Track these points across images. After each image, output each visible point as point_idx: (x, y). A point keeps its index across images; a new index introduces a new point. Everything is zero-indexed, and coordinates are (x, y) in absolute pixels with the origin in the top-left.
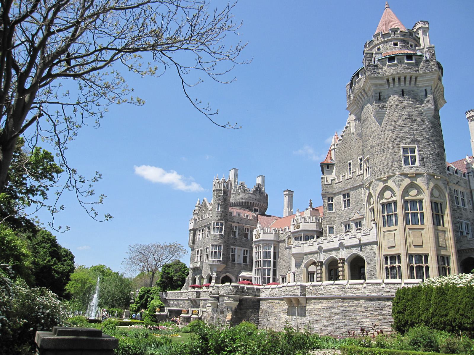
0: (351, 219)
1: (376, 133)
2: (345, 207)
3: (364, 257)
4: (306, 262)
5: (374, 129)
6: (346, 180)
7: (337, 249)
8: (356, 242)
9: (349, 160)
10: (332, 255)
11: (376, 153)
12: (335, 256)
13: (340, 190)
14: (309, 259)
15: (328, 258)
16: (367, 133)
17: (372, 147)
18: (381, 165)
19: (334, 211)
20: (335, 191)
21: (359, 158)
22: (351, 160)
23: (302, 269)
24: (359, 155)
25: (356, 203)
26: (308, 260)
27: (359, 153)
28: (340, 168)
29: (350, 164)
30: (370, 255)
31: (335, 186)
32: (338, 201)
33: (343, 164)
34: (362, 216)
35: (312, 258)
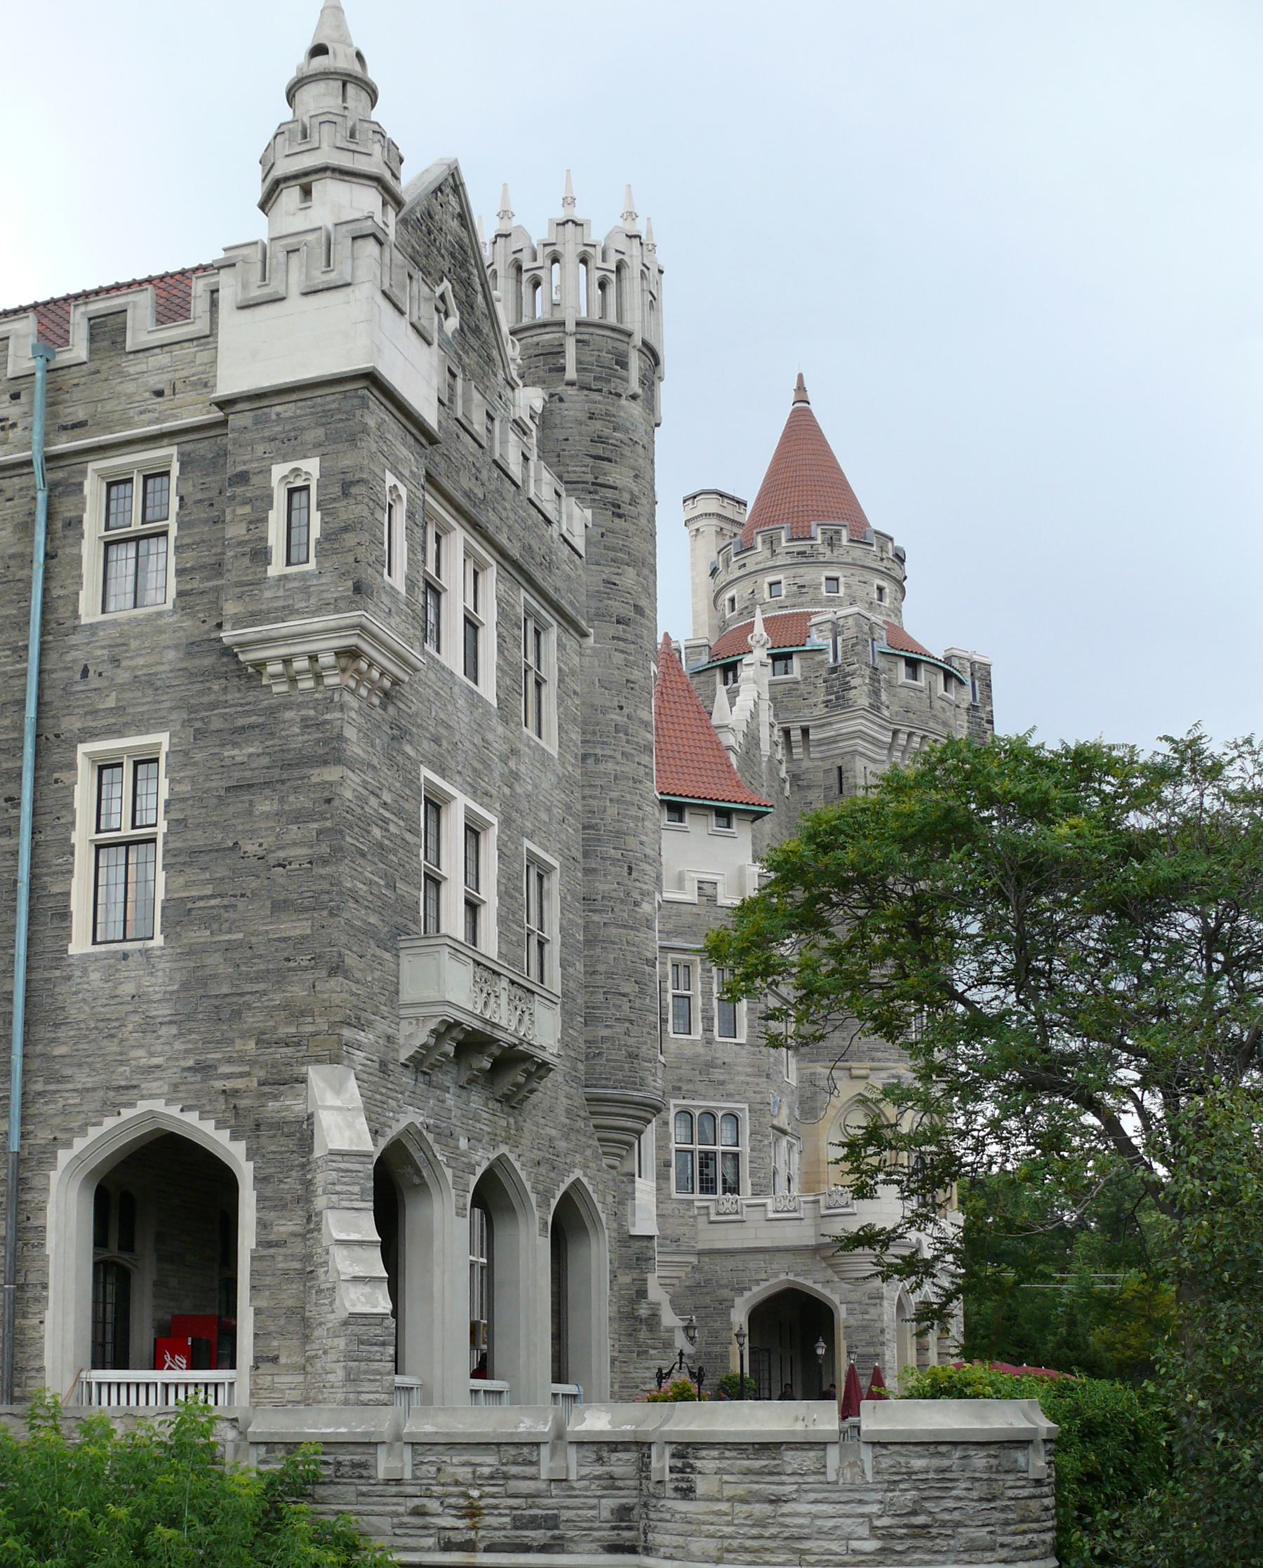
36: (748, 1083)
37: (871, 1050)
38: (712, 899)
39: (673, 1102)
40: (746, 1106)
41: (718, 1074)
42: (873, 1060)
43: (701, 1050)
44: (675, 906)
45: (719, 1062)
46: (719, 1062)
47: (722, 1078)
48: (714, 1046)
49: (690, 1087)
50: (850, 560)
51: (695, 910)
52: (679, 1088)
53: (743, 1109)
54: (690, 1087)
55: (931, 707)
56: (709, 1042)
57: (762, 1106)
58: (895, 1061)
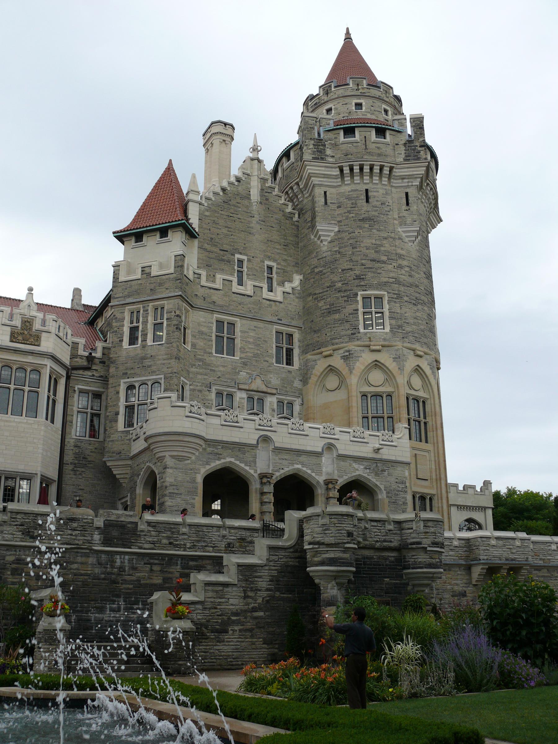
0: (242, 386)
1: (405, 263)
2: (220, 351)
3: (382, 487)
4: (213, 465)
5: (402, 252)
6: (234, 293)
7: (318, 455)
8: (366, 451)
9: (241, 254)
10: (299, 466)
11: (406, 298)
12: (309, 472)
13: (212, 307)
14: (223, 461)
15: (286, 469)
16: (382, 249)
17: (397, 282)
18: (414, 324)
19: (189, 347)
20: (198, 302)
21: (267, 263)
22: (247, 255)
23: (194, 481)
24: (270, 259)
25: (256, 355)
26: (218, 462)
27: (270, 254)
28: (213, 256)
29: (240, 262)
30: (394, 486)
31: (201, 292)
32: (204, 329)
33: (222, 253)
34: (274, 391)
35: (232, 460)
36: (164, 364)
37: (332, 339)
38: (149, 274)
39: (122, 381)
40: (162, 376)
41: (147, 362)
42: (333, 344)
43: (139, 351)
44: (130, 282)
45: (149, 356)
46: (149, 356)
47: (150, 364)
48: (146, 348)
49: (132, 371)
50: (337, 96)
51: (139, 282)
52: (126, 373)
53: (161, 379)
54: (132, 371)
55: (366, 149)
56: (144, 346)
57: (171, 375)
58: (346, 343)
